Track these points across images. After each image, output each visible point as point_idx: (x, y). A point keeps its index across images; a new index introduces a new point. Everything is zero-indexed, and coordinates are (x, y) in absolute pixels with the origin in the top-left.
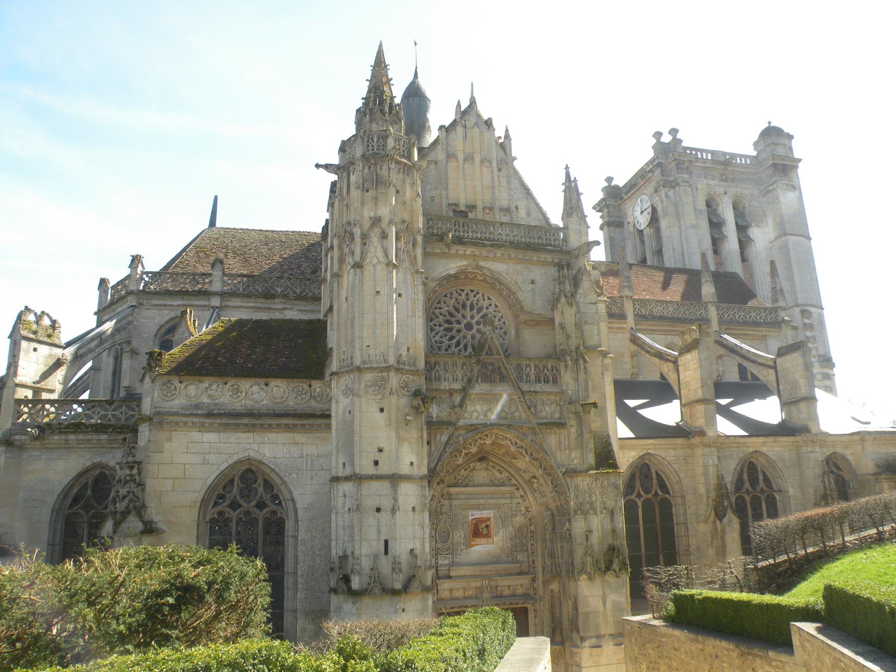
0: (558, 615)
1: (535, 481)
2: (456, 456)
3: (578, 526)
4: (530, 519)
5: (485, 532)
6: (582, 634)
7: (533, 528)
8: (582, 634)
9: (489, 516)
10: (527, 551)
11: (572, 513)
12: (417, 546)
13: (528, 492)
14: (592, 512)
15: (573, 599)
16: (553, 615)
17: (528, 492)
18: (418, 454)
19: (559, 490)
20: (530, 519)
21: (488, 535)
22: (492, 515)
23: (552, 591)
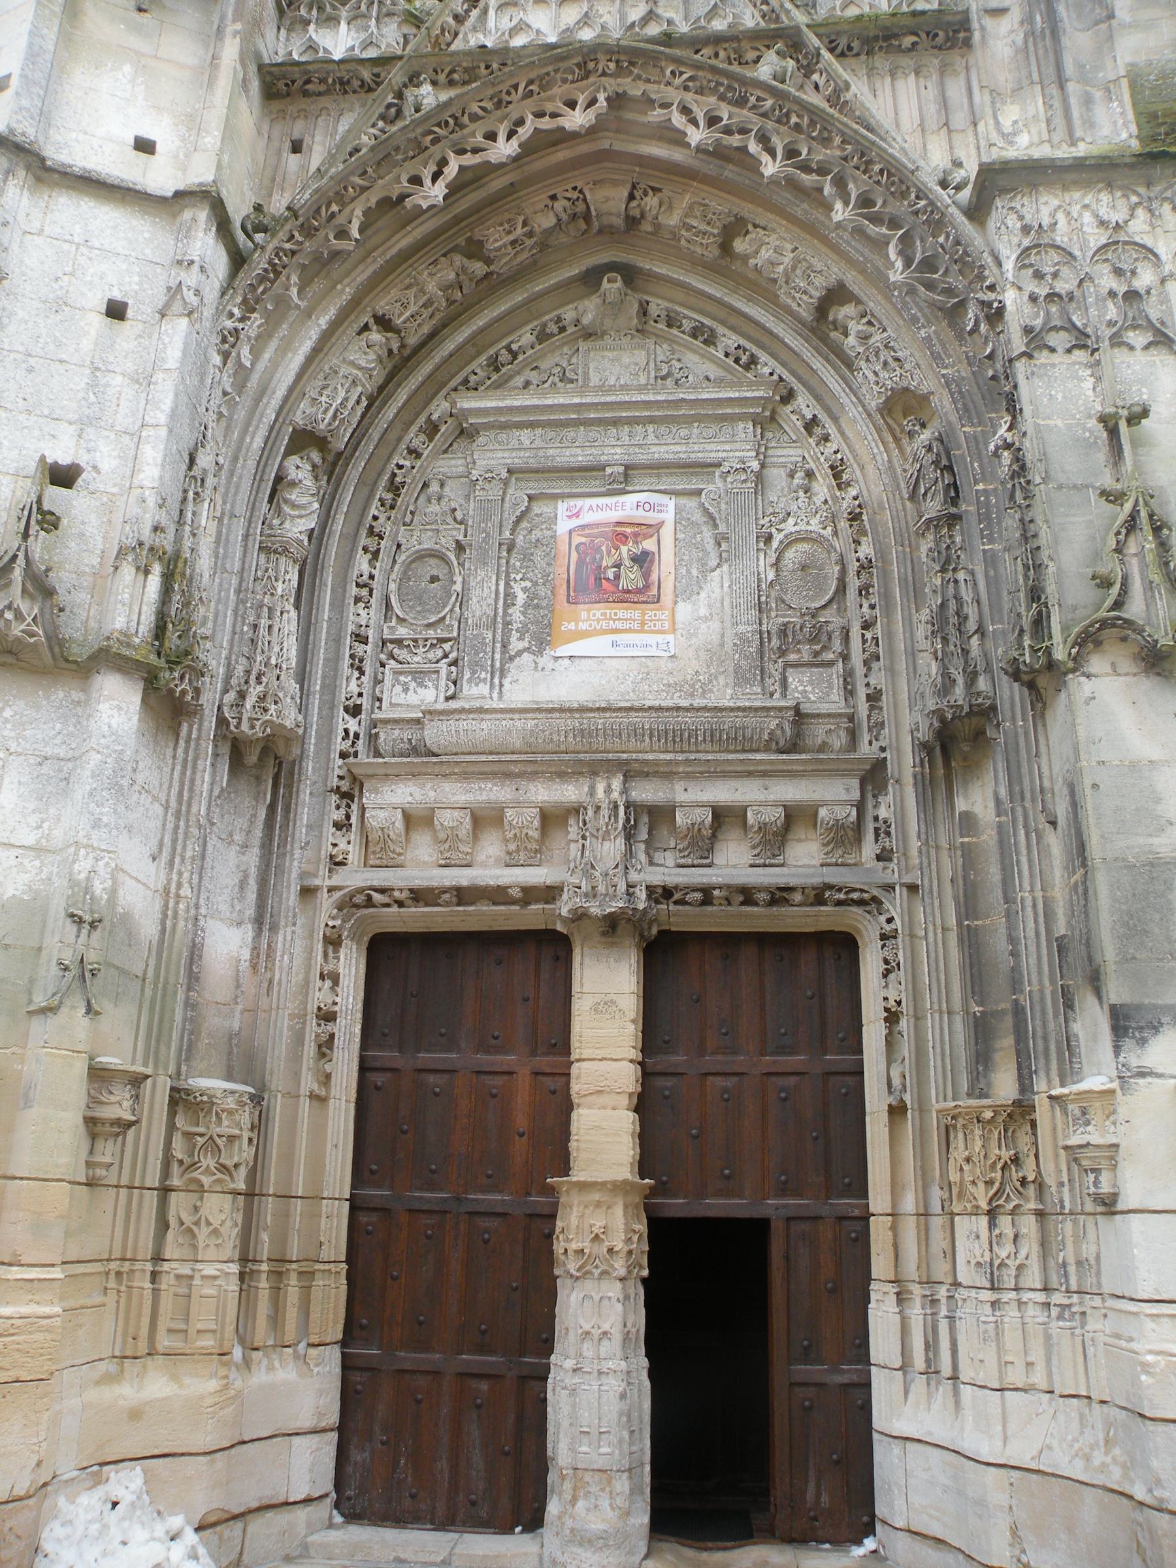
0: (1000, 944)
1: (845, 312)
2: (416, 180)
3: (1059, 398)
4: (854, 517)
5: (631, 577)
6: (1117, 991)
7: (866, 549)
8: (1117, 991)
9: (652, 517)
10: (845, 657)
11: (1018, 344)
12: (103, 459)
13: (834, 383)
14: (1138, 339)
15: (1061, 809)
16: (972, 942)
17: (834, 383)
18: (192, 123)
19: (953, 295)
20: (854, 517)
21: (643, 595)
22: (669, 516)
23: (968, 822)
